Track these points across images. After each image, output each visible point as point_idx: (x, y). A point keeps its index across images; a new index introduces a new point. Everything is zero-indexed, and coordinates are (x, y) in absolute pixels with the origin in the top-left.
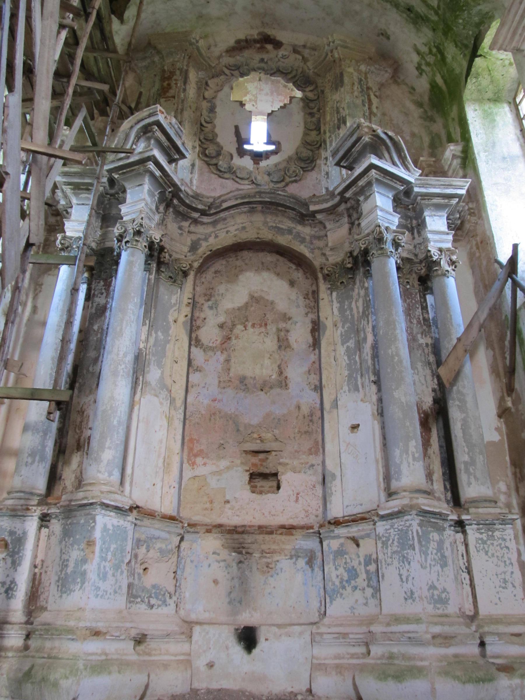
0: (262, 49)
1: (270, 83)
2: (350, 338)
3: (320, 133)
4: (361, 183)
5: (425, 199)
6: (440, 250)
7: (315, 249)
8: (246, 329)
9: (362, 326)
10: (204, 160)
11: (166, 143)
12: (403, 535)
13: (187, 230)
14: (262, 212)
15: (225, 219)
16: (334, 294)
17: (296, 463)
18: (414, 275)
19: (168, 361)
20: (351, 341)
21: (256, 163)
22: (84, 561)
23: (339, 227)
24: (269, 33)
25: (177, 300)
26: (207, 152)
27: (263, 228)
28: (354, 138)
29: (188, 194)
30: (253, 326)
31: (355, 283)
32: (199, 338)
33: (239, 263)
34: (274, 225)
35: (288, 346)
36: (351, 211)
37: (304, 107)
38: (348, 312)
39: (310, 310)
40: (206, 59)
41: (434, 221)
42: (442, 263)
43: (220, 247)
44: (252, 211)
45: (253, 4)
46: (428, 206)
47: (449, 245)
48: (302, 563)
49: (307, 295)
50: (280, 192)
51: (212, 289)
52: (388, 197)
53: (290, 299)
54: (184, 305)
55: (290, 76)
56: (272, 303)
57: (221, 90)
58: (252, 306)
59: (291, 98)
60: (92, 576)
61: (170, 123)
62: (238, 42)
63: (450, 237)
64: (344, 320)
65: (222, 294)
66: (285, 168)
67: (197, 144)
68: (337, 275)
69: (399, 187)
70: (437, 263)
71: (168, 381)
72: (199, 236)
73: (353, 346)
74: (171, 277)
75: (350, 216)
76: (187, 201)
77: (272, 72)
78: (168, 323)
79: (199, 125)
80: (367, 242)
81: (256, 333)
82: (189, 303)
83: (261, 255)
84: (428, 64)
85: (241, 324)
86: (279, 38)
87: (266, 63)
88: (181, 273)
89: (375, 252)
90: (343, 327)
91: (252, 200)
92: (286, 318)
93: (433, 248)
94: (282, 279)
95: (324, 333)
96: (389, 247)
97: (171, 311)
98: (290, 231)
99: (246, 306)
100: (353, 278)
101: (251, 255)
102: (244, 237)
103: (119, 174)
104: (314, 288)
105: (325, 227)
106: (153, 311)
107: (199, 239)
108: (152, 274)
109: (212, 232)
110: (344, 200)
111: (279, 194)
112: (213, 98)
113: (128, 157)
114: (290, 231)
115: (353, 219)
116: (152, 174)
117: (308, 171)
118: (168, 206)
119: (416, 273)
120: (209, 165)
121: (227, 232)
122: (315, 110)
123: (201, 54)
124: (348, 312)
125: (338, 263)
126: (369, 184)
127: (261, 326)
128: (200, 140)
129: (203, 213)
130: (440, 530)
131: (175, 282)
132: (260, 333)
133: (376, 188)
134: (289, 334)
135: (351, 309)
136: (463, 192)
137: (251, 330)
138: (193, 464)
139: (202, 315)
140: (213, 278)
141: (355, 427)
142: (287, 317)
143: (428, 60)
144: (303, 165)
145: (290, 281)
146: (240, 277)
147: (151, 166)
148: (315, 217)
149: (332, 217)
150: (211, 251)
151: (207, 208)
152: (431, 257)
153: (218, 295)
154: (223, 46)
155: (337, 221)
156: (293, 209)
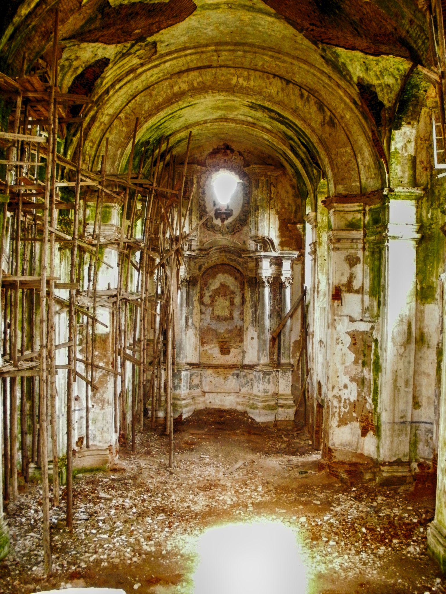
12: (259, 376)
17: (235, 345)
19: (194, 315)
21: (223, 220)
22: (179, 383)
33: (216, 270)
44: (221, 252)
47: (289, 276)
48: (235, 377)
60: (182, 387)
62: (214, 150)
63: (290, 272)
70: (284, 283)
71: (195, 323)
86: (233, 147)
92: (233, 293)
93: (283, 278)
96: (266, 284)
99: (219, 288)
114: (235, 260)
130: (269, 375)
136: (296, 256)
138: (203, 346)
141: (252, 338)
146: (217, 276)
154: (207, 153)
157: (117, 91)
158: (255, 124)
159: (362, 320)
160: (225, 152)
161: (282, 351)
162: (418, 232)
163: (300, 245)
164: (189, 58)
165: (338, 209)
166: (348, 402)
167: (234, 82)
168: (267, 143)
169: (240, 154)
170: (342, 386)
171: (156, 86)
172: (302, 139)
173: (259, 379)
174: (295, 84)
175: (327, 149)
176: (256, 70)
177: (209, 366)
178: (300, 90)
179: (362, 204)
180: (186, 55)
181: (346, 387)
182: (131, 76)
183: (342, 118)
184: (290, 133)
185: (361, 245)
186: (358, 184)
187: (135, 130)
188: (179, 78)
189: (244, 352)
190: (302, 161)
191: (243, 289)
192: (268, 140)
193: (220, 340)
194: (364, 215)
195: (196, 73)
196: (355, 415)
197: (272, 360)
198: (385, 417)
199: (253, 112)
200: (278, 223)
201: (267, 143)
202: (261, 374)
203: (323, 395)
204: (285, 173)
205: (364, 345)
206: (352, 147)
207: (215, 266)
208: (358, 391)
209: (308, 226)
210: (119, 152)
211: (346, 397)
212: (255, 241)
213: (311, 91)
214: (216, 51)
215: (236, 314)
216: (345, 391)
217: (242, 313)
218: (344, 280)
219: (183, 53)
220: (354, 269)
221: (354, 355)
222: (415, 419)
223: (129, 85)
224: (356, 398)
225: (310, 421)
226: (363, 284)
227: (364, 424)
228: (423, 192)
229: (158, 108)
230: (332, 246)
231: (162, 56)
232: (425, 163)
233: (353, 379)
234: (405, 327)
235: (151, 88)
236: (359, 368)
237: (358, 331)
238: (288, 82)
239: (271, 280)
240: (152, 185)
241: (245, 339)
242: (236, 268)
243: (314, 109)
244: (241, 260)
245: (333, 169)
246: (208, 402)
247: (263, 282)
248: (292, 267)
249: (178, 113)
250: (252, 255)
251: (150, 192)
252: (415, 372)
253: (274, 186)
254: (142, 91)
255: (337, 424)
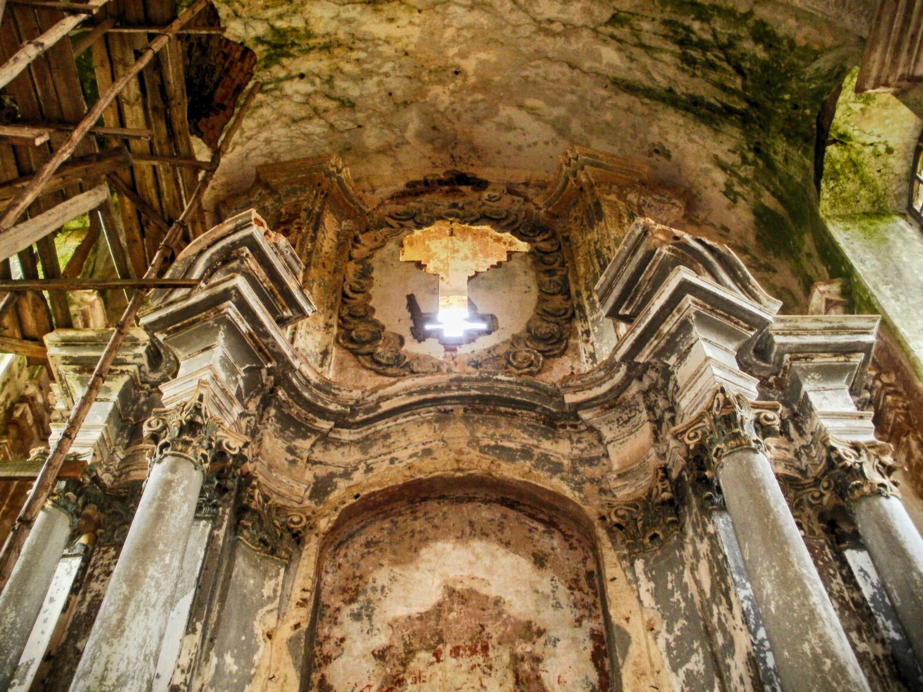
0: (453, 192)
1: (470, 238)
2: (692, 651)
3: (569, 297)
4: (667, 327)
5: (798, 359)
7: (584, 482)
8: (438, 661)
9: (715, 620)
10: (346, 348)
11: (268, 284)
13: (305, 455)
14: (466, 419)
15: (387, 436)
16: (639, 564)
18: (808, 511)
20: (694, 658)
23: (631, 433)
24: (465, 171)
25: (275, 591)
26: (353, 334)
27: (467, 450)
28: (640, 254)
29: (308, 381)
30: (456, 652)
31: (683, 533)
32: (329, 681)
33: (418, 525)
34: (493, 443)
36: (652, 396)
37: (534, 263)
38: (677, 596)
39: (587, 613)
40: (356, 200)
41: (825, 398)
42: (866, 471)
43: (377, 489)
44: (444, 417)
45: (434, 128)
46: (807, 372)
49: (576, 581)
50: (500, 377)
51: (361, 577)
52: (726, 350)
53: (537, 591)
54: (293, 604)
55: (504, 224)
56: (497, 602)
57: (382, 247)
58: (451, 610)
59: (510, 254)
61: (276, 245)
62: (411, 184)
63: (869, 423)
64: (670, 614)
65: (383, 587)
66: (508, 353)
67: (334, 321)
68: (640, 524)
69: (744, 331)
72: (331, 469)
73: (701, 667)
74: (262, 541)
75: (650, 408)
76: (306, 395)
77: (472, 219)
78: (252, 635)
79: (339, 293)
80: (699, 432)
81: (465, 667)
82: (305, 600)
83: (467, 508)
84: (744, 181)
85: (427, 650)
87: (462, 208)
88: (287, 536)
89: (722, 446)
90: (670, 630)
91: (442, 395)
94: (516, 552)
95: (625, 653)
97: (261, 612)
98: (526, 453)
100: (679, 524)
101: (445, 509)
102: (428, 469)
103: (168, 333)
104: (591, 565)
105: (600, 440)
106: (216, 608)
107: (332, 475)
108: (220, 527)
109: (360, 462)
110: (635, 372)
111: (497, 380)
112: (368, 258)
113: (188, 297)
114: (526, 453)
115: (658, 412)
116: (232, 329)
117: (554, 356)
118: (265, 404)
119: (811, 506)
120: (356, 354)
121: (392, 461)
122: (556, 265)
123: (346, 192)
124: (677, 596)
125: (639, 499)
126: (685, 326)
127: (474, 652)
128: (340, 317)
129: (341, 421)
131: (273, 552)
132: (473, 667)
133: (697, 332)
134: (541, 666)
135: (684, 588)
137: (450, 662)
139: (337, 633)
140: (363, 557)
142: (535, 629)
143: (743, 174)
144: (542, 347)
145: (534, 555)
146: (424, 552)
147: (230, 309)
148: (578, 418)
149: (613, 415)
150: (357, 496)
151: (348, 410)
152: (840, 459)
153: (374, 589)
154: (385, 192)
155: (626, 422)
156: (531, 407)
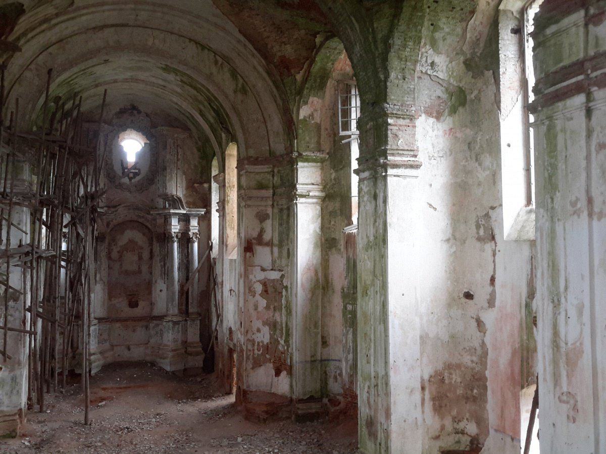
6: (193, 233)
21: (130, 179)
35: (142, 258)
44: (129, 209)
47: (197, 231)
62: (121, 109)
63: (198, 228)
70: (192, 238)
86: (141, 108)
92: (142, 248)
93: (191, 233)
98: (143, 217)
114: (143, 217)
136: (203, 213)
141: (161, 291)
154: (113, 112)
157: (28, 41)
158: (164, 87)
159: (272, 270)
160: (132, 112)
161: (190, 301)
162: (322, 191)
163: (207, 204)
164: (107, 13)
165: (249, 170)
166: (261, 344)
167: (150, 43)
168: (176, 106)
169: (147, 115)
170: (255, 329)
171: (69, 39)
172: (212, 104)
173: (169, 329)
174: (210, 49)
175: (239, 115)
176: (172, 33)
177: (118, 320)
178: (215, 56)
179: (272, 166)
180: (104, 11)
181: (259, 330)
182: (45, 26)
183: (254, 86)
184: (200, 98)
185: (271, 203)
186: (268, 148)
187: (48, 85)
188: (95, 34)
189: (152, 304)
190: (211, 126)
191: (151, 244)
192: (177, 104)
193: (128, 293)
194: (273, 176)
195: (112, 29)
196: (268, 356)
197: (179, 309)
198: (296, 357)
199: (165, 75)
200: (184, 182)
201: (176, 106)
202: (171, 324)
203: (235, 341)
204: (191, 136)
205: (275, 291)
206: (263, 114)
207: (123, 223)
208: (270, 334)
209: (214, 186)
210: (30, 106)
211: (259, 340)
212: (164, 199)
213: (226, 59)
214: (134, 10)
215: (145, 268)
216: (258, 335)
217: (150, 267)
218: (255, 234)
219: (99, 9)
220: (264, 225)
221: (266, 301)
222: (324, 358)
223: (41, 35)
224: (268, 341)
225: (220, 366)
226: (272, 237)
227: (278, 365)
228: (327, 156)
229: (71, 64)
230: (243, 204)
231: (79, 9)
232: (329, 130)
233: (265, 323)
234: (313, 274)
235: (64, 41)
236: (271, 313)
237: (269, 280)
238: (203, 47)
239: (180, 235)
240: (66, 142)
241: (153, 292)
242: (144, 225)
243: (227, 75)
244: (150, 216)
245: (244, 134)
246: (116, 355)
247: (173, 237)
248: (199, 224)
249: (90, 69)
250: (161, 212)
251: (65, 149)
252: (323, 314)
253: (180, 148)
254: (54, 44)
255: (251, 366)
